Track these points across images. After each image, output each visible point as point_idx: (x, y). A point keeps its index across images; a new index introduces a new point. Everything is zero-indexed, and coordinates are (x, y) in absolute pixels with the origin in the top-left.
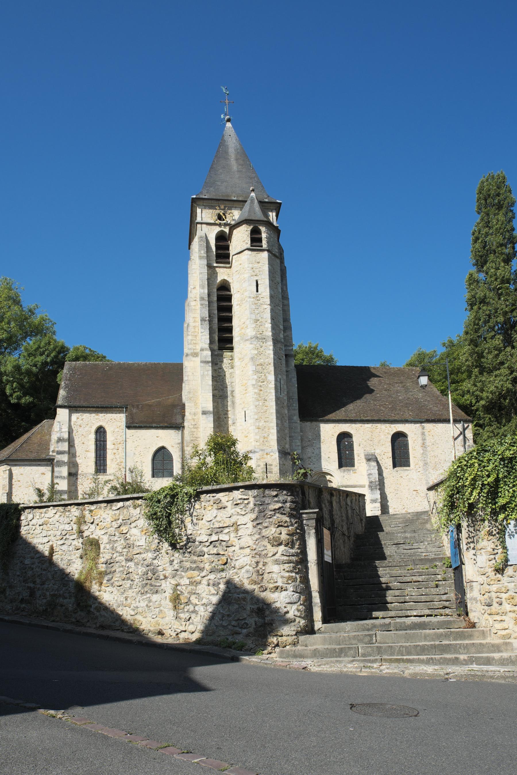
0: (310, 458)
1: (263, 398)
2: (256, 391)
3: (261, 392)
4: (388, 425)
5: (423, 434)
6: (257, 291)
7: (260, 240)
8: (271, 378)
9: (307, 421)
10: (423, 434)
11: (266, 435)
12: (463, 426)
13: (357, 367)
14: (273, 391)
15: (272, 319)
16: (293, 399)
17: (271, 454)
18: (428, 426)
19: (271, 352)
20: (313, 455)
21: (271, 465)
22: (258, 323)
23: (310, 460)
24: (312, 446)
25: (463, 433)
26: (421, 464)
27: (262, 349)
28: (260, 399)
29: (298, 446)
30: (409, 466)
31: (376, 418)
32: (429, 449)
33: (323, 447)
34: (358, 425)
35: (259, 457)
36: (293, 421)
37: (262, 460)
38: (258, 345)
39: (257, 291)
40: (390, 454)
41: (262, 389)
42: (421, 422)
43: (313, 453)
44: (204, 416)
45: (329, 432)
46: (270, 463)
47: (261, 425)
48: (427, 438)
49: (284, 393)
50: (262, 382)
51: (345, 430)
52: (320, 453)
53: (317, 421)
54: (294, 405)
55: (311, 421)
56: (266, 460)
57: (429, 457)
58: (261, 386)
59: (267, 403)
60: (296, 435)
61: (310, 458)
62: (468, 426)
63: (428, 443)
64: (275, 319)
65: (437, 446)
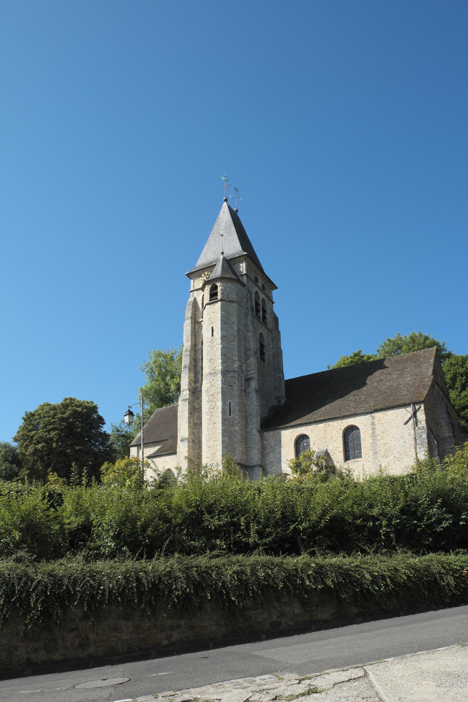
2: (208, 417)
3: (212, 417)
4: (339, 421)
5: (373, 424)
6: (213, 336)
7: (216, 294)
8: (220, 404)
9: (270, 430)
10: (373, 424)
11: (214, 452)
12: (415, 408)
13: (323, 372)
14: (220, 415)
15: (224, 355)
18: (378, 415)
19: (220, 383)
20: (274, 459)
24: (274, 451)
25: (415, 415)
26: (371, 453)
27: (214, 382)
28: (211, 423)
29: (256, 454)
30: (361, 457)
31: (327, 417)
32: (378, 437)
33: (283, 451)
34: (313, 427)
38: (211, 379)
39: (213, 336)
40: (341, 448)
41: (213, 414)
42: (371, 413)
45: (288, 436)
47: (211, 444)
48: (377, 427)
49: (234, 413)
50: (213, 409)
51: (302, 433)
52: (281, 456)
53: (277, 429)
55: (274, 430)
57: (378, 445)
58: (212, 413)
59: (216, 425)
60: (254, 445)
62: (420, 407)
63: (377, 432)
64: (227, 355)
65: (387, 433)
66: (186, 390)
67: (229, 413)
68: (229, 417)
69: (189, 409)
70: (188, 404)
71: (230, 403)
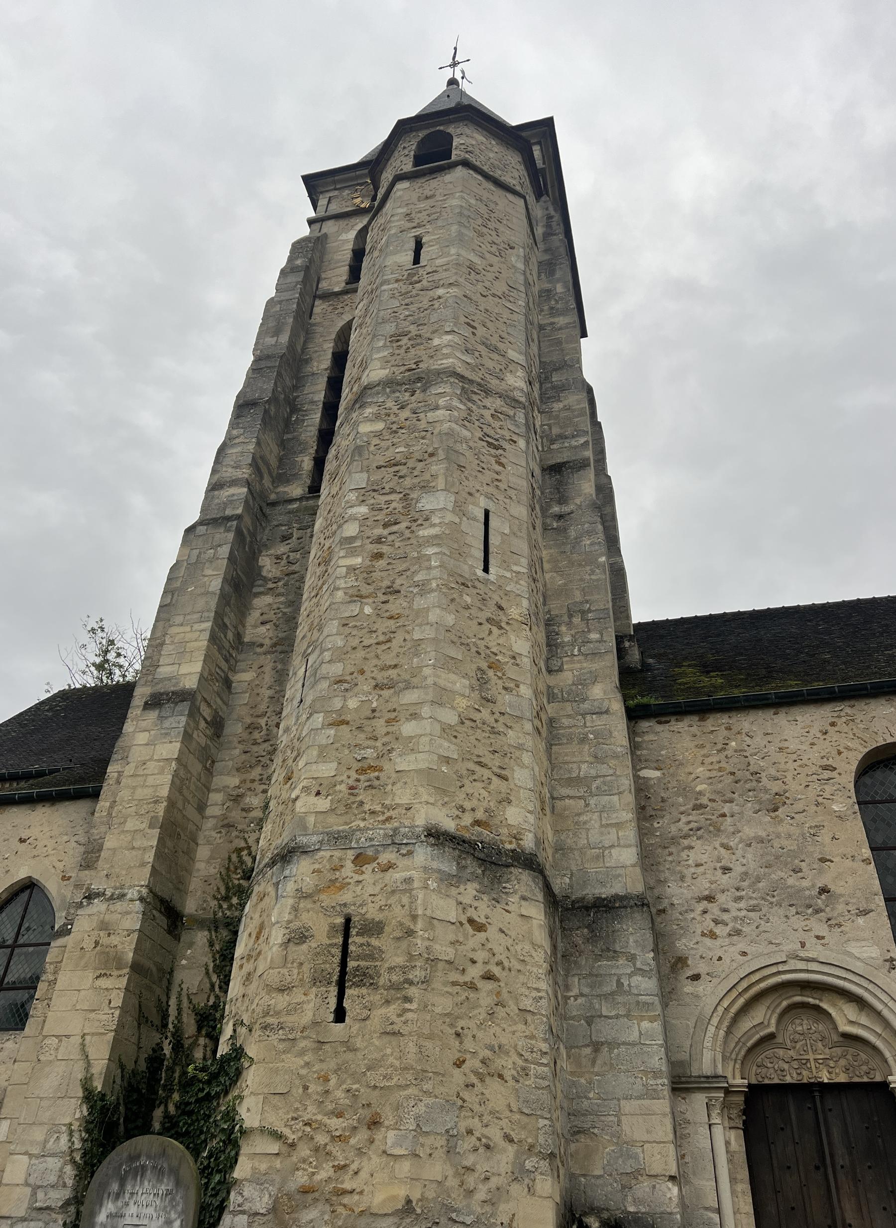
0: (710, 898)
1: (386, 583)
3: (382, 563)
6: (416, 260)
16: (583, 613)
17: (387, 856)
20: (725, 880)
21: (374, 928)
22: (405, 341)
23: (714, 908)
28: (366, 590)
29: (618, 825)
35: (309, 882)
36: (586, 706)
37: (327, 899)
38: (390, 404)
41: (385, 549)
43: (726, 870)
44: (153, 715)
46: (372, 912)
47: (352, 703)
50: (386, 526)
54: (594, 636)
56: (347, 896)
58: (379, 540)
61: (710, 898)
66: (234, 483)
67: (481, 555)
68: (480, 573)
69: (231, 559)
70: (231, 536)
71: (487, 513)
